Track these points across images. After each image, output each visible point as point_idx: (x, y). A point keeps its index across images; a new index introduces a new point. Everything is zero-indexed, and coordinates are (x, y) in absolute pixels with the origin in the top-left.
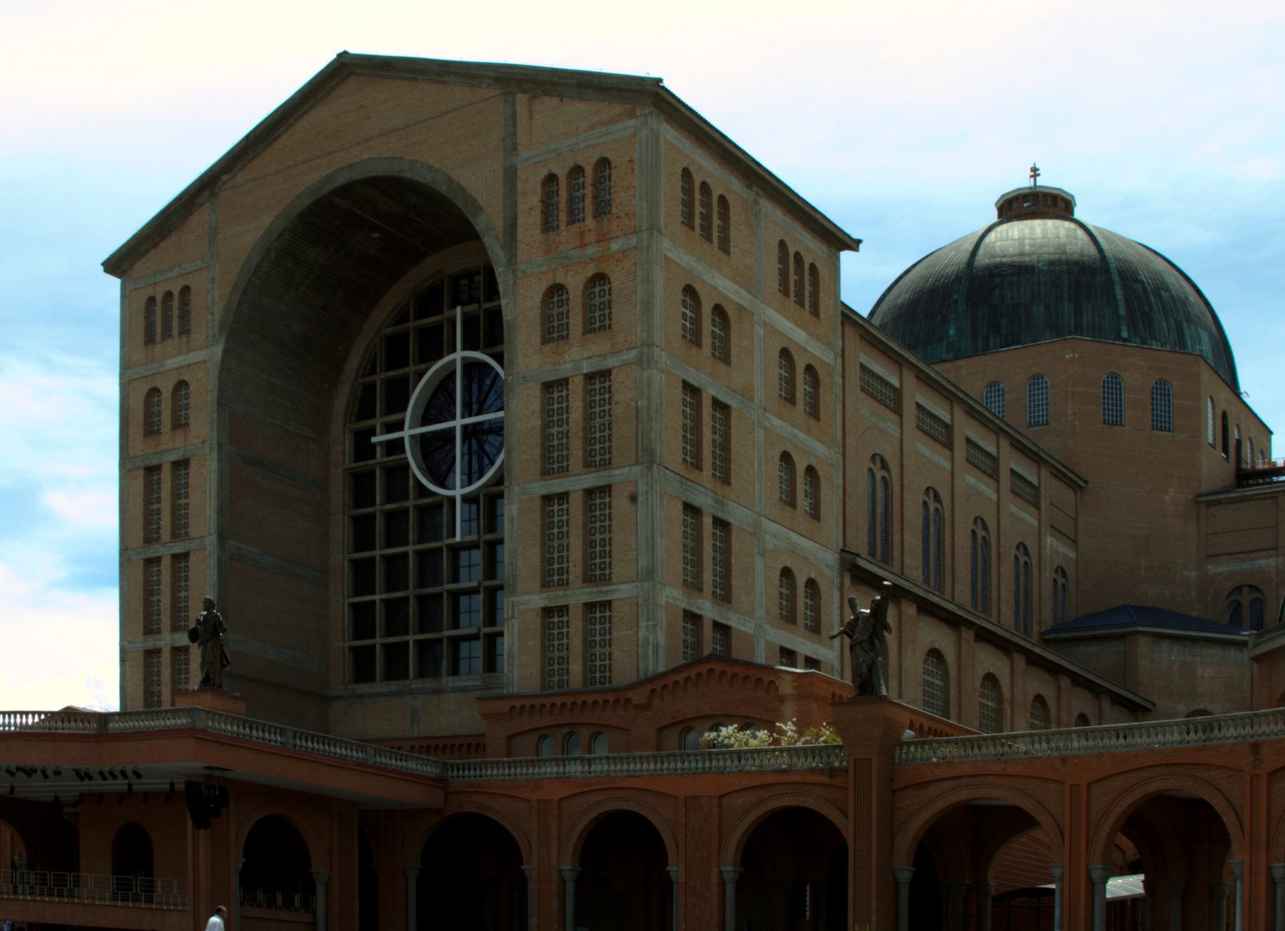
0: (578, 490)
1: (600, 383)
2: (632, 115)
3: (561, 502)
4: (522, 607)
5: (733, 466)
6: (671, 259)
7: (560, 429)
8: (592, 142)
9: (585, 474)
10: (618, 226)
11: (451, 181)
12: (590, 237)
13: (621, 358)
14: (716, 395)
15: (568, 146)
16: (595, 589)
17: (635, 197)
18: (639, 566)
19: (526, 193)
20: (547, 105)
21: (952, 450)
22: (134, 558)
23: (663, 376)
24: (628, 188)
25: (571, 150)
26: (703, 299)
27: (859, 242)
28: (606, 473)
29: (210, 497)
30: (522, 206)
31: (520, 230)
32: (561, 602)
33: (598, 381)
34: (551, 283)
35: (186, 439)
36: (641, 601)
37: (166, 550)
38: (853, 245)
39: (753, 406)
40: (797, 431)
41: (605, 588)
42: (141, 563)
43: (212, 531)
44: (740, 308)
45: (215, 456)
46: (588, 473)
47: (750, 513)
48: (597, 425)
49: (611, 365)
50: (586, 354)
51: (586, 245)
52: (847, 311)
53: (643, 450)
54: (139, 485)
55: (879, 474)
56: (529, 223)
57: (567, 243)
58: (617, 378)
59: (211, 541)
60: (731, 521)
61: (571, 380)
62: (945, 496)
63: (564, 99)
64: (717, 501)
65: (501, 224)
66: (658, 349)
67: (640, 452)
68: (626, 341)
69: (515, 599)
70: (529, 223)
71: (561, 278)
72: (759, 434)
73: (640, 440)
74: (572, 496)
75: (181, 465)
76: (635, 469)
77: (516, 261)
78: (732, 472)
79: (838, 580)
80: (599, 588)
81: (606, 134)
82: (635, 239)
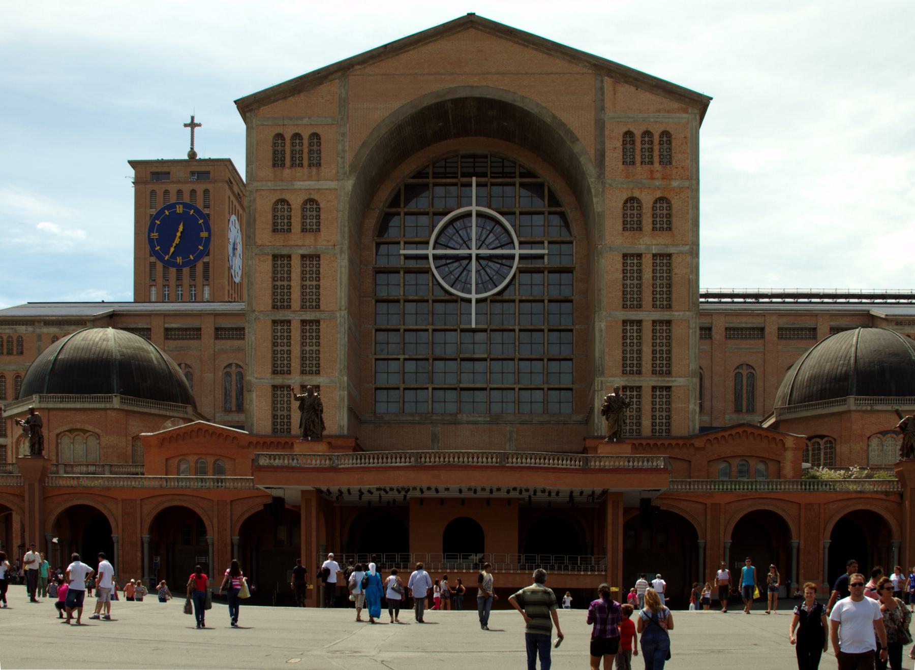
0: (649, 320)
1: (660, 259)
2: (686, 111)
3: (632, 324)
4: (608, 384)
7: (632, 282)
8: (659, 120)
10: (677, 173)
11: (554, 117)
12: (659, 175)
13: (679, 249)
15: (642, 118)
16: (660, 379)
17: (688, 159)
18: (690, 369)
19: (611, 138)
20: (625, 90)
22: (262, 318)
24: (683, 153)
25: (644, 121)
28: (668, 313)
29: (341, 285)
30: (608, 145)
31: (607, 159)
32: (637, 384)
33: (658, 258)
34: (630, 196)
36: (690, 388)
37: (296, 317)
41: (667, 379)
42: (270, 323)
43: (343, 308)
45: (346, 256)
48: (658, 284)
49: (672, 252)
50: (654, 242)
51: (654, 179)
53: (693, 304)
54: (265, 267)
56: (613, 157)
57: (641, 174)
58: (676, 260)
59: (342, 316)
61: (644, 255)
63: (639, 89)
65: (593, 152)
67: (691, 305)
68: (682, 240)
69: (603, 379)
70: (613, 157)
71: (636, 194)
73: (691, 297)
74: (644, 324)
75: (312, 258)
76: (688, 313)
77: (604, 177)
80: (663, 379)
81: (669, 118)
82: (688, 183)
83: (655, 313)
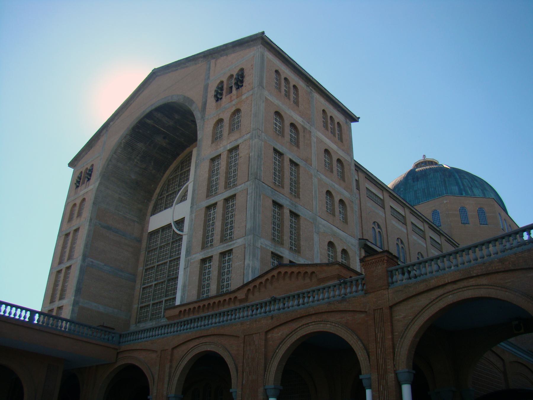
0: (222, 200)
5: (301, 190)
6: (268, 99)
9: (225, 192)
13: (244, 138)
14: (292, 158)
21: (406, 225)
23: (263, 143)
26: (285, 119)
27: (359, 118)
35: (80, 220)
38: (357, 119)
39: (311, 167)
40: (334, 184)
44: (304, 129)
46: (226, 191)
47: (311, 213)
52: (357, 164)
53: (251, 174)
55: (377, 230)
60: (300, 214)
62: (405, 241)
64: (292, 204)
66: (260, 132)
72: (315, 181)
73: (250, 170)
78: (301, 193)
79: (359, 252)
83: (226, 192)
